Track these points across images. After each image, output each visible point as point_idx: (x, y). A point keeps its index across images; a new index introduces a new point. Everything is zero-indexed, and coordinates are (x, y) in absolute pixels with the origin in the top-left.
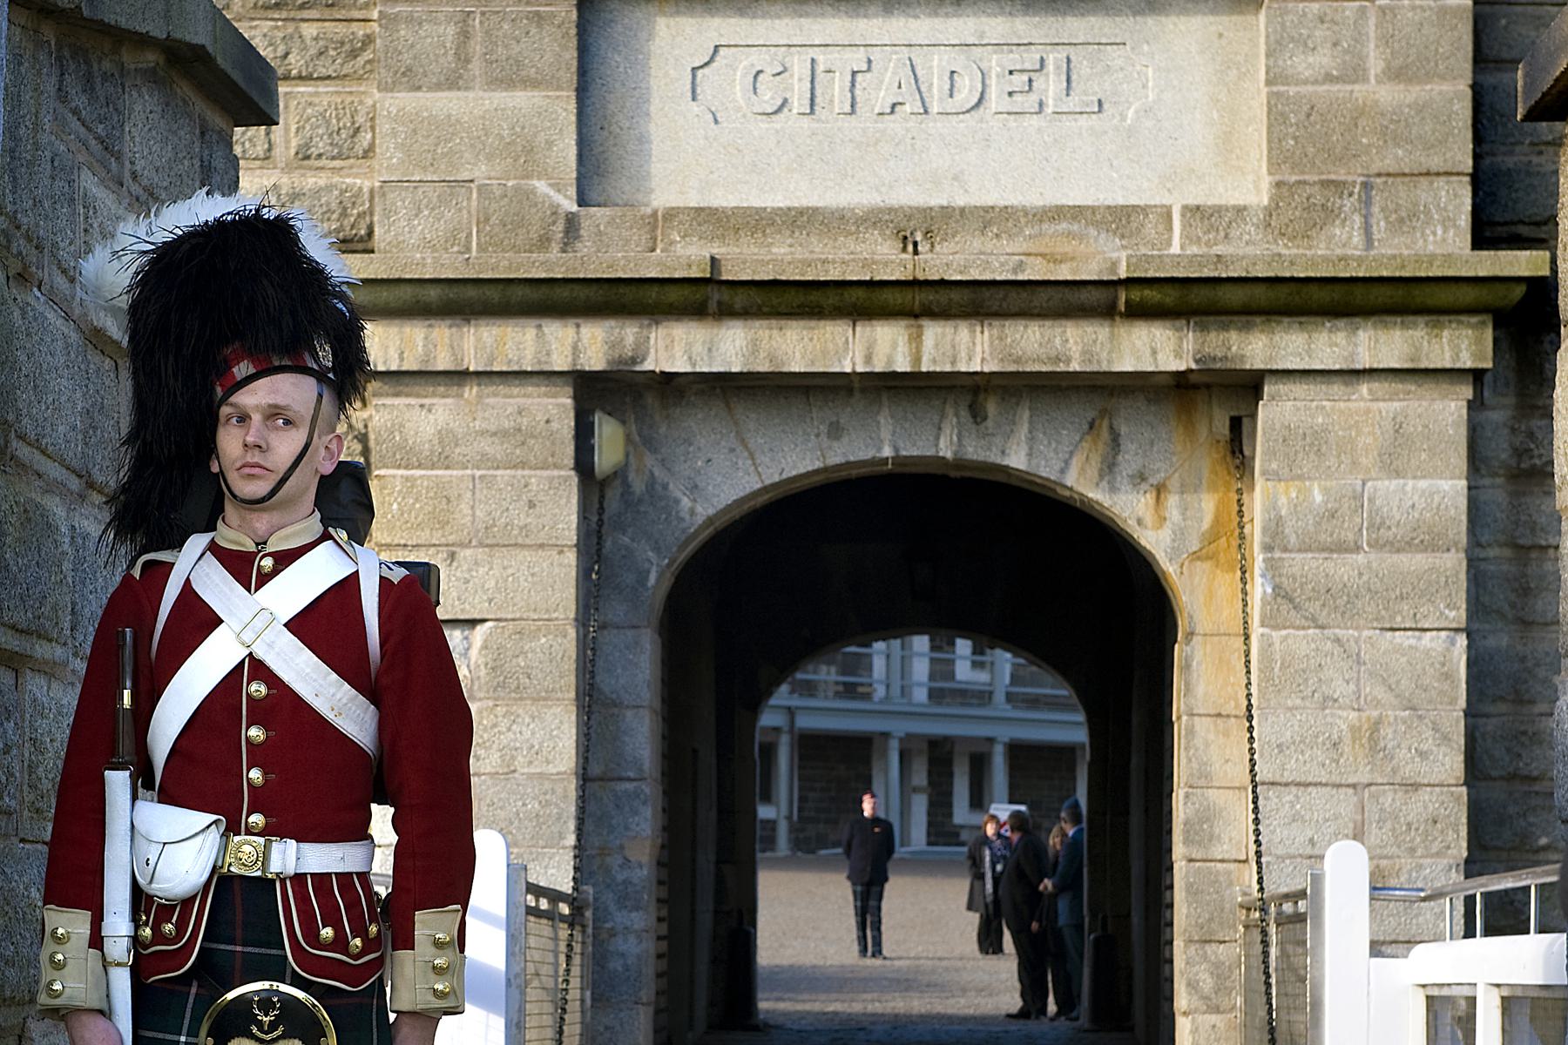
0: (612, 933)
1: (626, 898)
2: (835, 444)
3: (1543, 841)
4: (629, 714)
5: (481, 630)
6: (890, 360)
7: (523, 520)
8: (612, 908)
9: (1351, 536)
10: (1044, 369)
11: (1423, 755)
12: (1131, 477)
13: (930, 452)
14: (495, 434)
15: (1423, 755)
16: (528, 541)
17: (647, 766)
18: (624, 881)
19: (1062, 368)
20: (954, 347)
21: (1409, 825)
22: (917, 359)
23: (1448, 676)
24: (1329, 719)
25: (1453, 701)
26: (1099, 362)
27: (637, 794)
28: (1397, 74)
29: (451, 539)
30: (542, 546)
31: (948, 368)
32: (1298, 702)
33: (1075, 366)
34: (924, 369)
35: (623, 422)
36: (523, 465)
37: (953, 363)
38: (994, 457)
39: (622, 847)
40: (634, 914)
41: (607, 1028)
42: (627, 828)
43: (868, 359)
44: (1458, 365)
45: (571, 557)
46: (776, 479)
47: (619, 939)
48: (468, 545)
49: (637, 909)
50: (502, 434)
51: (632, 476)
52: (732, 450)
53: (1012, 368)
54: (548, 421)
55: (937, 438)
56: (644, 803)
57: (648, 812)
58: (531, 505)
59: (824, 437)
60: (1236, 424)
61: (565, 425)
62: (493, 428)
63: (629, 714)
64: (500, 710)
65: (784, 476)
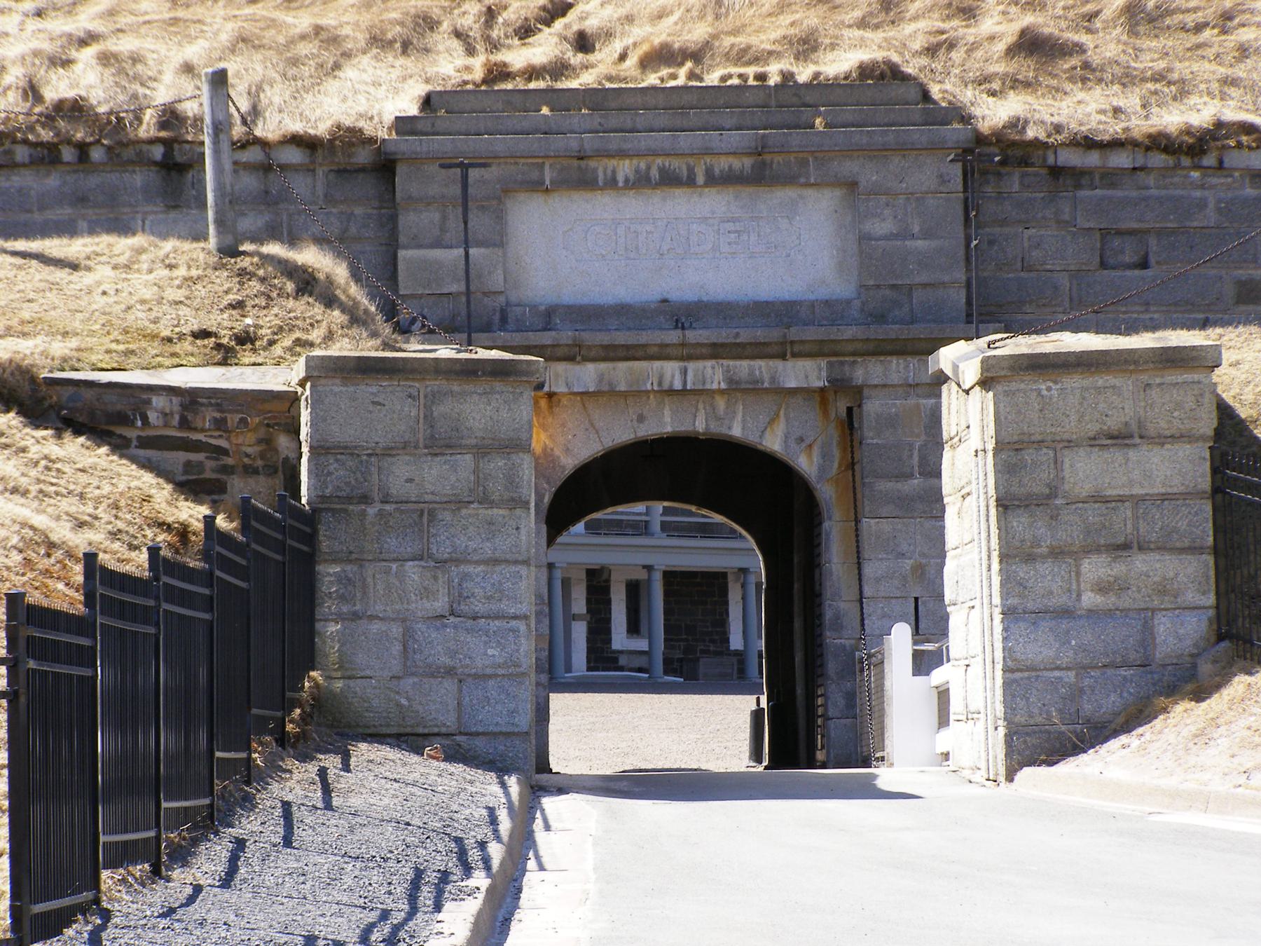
6: (672, 383)
13: (691, 429)
22: (685, 383)
28: (927, 234)
33: (766, 385)
37: (704, 384)
38: (724, 430)
43: (660, 384)
59: (635, 423)
60: (850, 410)
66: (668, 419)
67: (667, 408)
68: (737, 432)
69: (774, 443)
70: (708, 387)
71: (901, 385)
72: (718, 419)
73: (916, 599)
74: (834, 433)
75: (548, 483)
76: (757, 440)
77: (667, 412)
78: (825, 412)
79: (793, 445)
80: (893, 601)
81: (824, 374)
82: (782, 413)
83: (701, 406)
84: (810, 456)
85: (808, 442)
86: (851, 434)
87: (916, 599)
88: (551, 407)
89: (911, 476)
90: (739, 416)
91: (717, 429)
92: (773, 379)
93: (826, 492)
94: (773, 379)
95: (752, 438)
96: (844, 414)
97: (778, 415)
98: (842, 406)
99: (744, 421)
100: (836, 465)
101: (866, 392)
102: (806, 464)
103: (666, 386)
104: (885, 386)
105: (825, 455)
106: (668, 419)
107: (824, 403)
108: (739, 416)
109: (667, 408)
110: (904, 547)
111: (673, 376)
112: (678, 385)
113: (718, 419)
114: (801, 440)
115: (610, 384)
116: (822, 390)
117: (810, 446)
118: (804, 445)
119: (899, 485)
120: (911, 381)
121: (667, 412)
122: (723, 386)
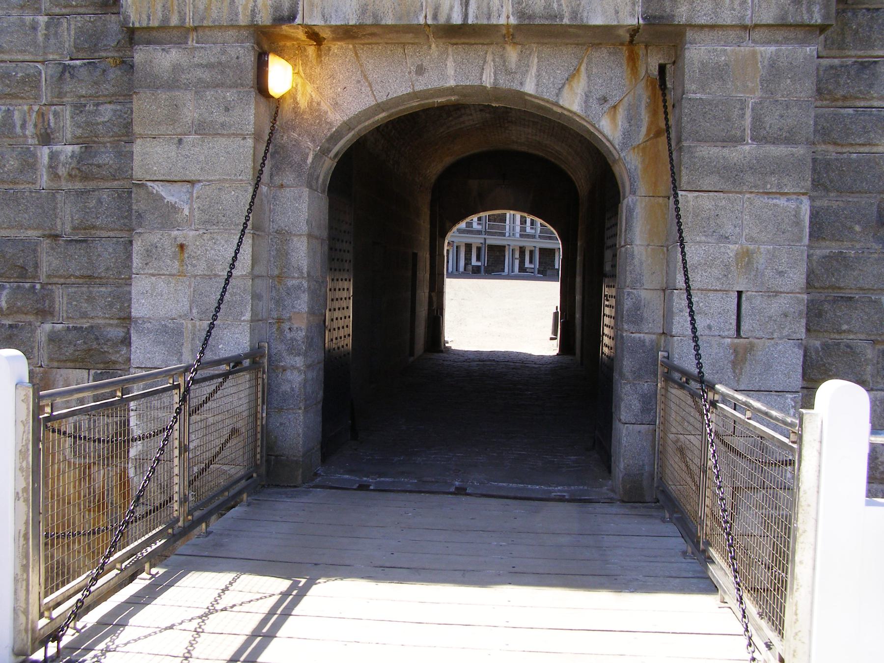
0: (284, 369)
1: (292, 350)
2: (420, 78)
3: (845, 327)
4: (295, 239)
5: (198, 186)
6: (449, 17)
7: (222, 119)
8: (284, 354)
9: (739, 134)
10: (547, 22)
11: (781, 273)
12: (599, 99)
14: (206, 66)
15: (781, 273)
16: (225, 132)
17: (305, 270)
18: (291, 339)
19: (558, 22)
20: (489, 8)
21: (770, 317)
22: (466, 16)
23: (798, 223)
24: (722, 250)
25: (800, 240)
26: (582, 19)
27: (299, 287)
29: (179, 130)
30: (235, 135)
31: (485, 22)
32: (703, 238)
33: (566, 21)
34: (470, 22)
35: (294, 66)
36: (221, 85)
38: (515, 86)
39: (290, 319)
40: (297, 358)
41: (281, 424)
42: (293, 307)
43: (435, 17)
44: (813, 22)
45: (250, 142)
46: (385, 99)
47: (288, 373)
48: (190, 134)
49: (299, 355)
50: (210, 66)
51: (299, 97)
52: (359, 82)
53: (526, 22)
54: (238, 58)
55: (481, 75)
56: (304, 292)
57: (305, 297)
58: (227, 109)
59: (413, 74)
60: (662, 69)
61: (249, 60)
62: (204, 62)
63: (295, 239)
64: (206, 237)
65: (389, 97)
66: (451, 71)
67: (451, 59)
68: (529, 88)
69: (572, 101)
70: (494, 21)
71: (732, 27)
72: (509, 72)
73: (740, 293)
74: (643, 93)
75: (313, 141)
76: (553, 99)
77: (450, 63)
78: (634, 69)
79: (595, 105)
80: (711, 294)
81: (639, 9)
82: (583, 68)
83: (489, 58)
84: (614, 119)
85: (612, 103)
86: (664, 95)
87: (740, 293)
88: (319, 56)
89: (742, 140)
90: (533, 71)
91: (504, 83)
92: (575, 14)
93: (630, 164)
94: (575, 14)
95: (549, 95)
96: (655, 72)
97: (578, 70)
98: (652, 62)
99: (538, 76)
100: (644, 130)
101: (689, 34)
102: (609, 129)
103: (442, 20)
104: (712, 27)
105: (631, 118)
106: (451, 71)
107: (633, 59)
108: (533, 71)
109: (451, 59)
110: (729, 229)
111: (451, 8)
112: (457, 19)
113: (509, 72)
114: (604, 100)
115: (375, 16)
116: (634, 31)
117: (615, 107)
118: (607, 106)
119: (726, 152)
120: (748, 22)
121: (450, 63)
122: (513, 21)
